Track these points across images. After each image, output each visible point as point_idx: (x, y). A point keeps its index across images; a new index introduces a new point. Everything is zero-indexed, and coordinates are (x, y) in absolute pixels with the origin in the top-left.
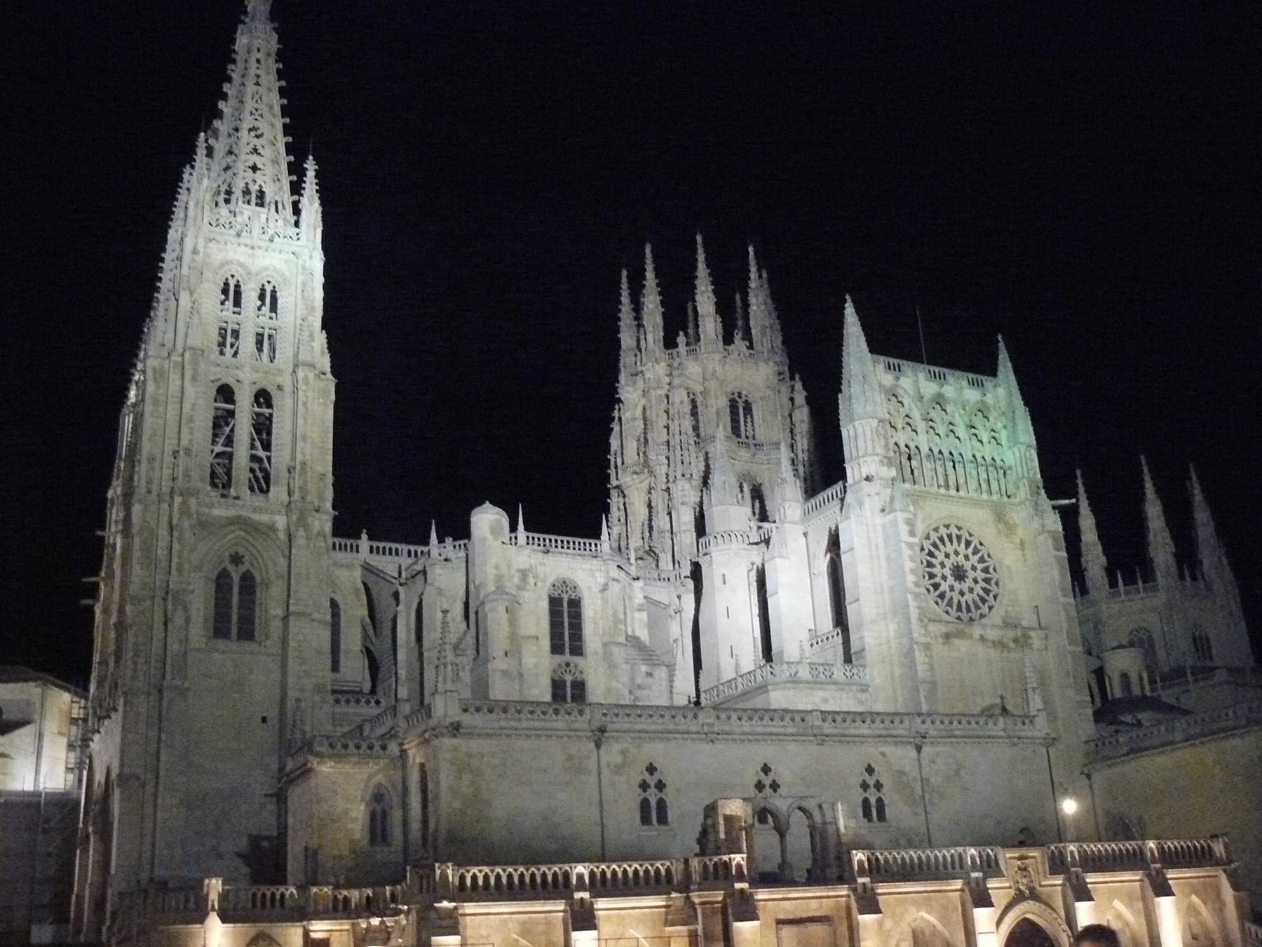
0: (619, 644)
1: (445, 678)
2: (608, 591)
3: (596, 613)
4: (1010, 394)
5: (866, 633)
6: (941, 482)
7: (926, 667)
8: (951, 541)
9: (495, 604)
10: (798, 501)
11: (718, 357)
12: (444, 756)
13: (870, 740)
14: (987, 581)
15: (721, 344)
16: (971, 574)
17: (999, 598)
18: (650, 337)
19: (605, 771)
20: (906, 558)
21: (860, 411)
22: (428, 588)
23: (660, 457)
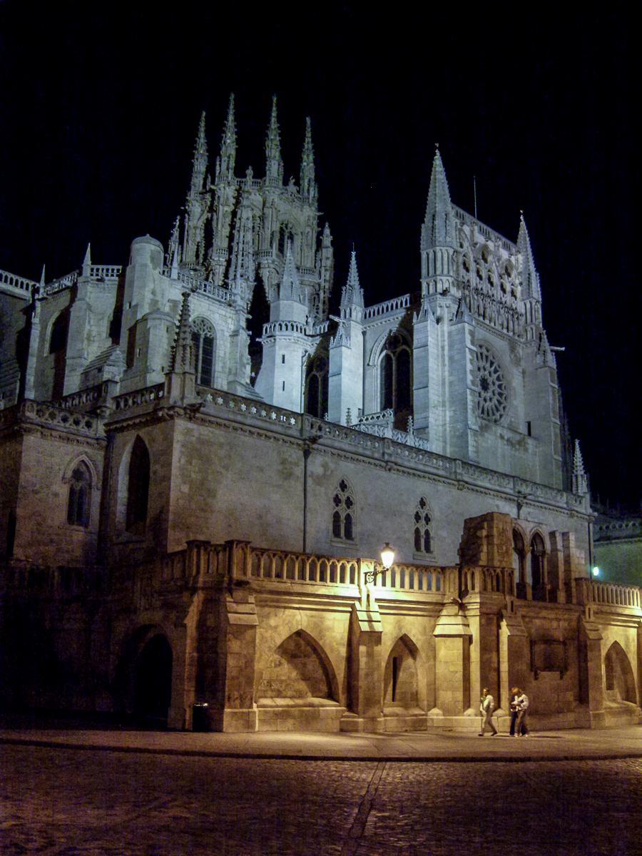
0: (242, 384)
1: (183, 360)
2: (239, 338)
3: (225, 354)
4: (526, 261)
5: (430, 415)
6: (482, 312)
7: (474, 449)
8: (482, 358)
9: (158, 322)
10: (361, 306)
11: (278, 192)
12: (178, 436)
13: (492, 493)
14: (500, 394)
15: (281, 183)
16: (491, 388)
17: (507, 410)
18: (224, 166)
19: (310, 481)
20: (468, 361)
21: (441, 239)
22: (77, 304)
23: (221, 259)
